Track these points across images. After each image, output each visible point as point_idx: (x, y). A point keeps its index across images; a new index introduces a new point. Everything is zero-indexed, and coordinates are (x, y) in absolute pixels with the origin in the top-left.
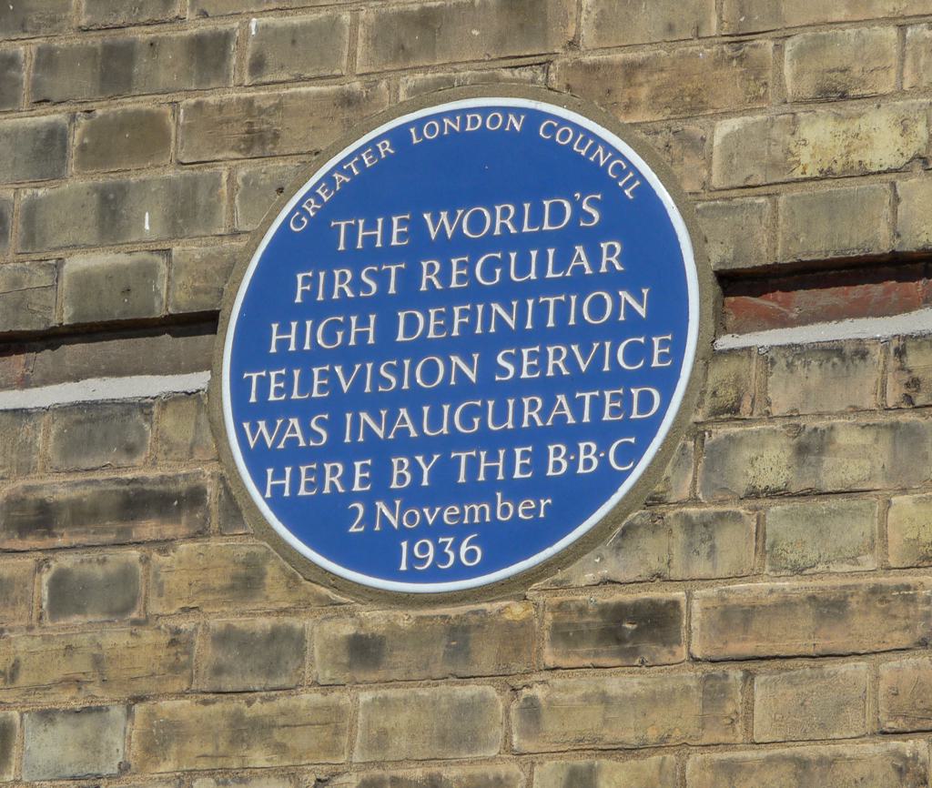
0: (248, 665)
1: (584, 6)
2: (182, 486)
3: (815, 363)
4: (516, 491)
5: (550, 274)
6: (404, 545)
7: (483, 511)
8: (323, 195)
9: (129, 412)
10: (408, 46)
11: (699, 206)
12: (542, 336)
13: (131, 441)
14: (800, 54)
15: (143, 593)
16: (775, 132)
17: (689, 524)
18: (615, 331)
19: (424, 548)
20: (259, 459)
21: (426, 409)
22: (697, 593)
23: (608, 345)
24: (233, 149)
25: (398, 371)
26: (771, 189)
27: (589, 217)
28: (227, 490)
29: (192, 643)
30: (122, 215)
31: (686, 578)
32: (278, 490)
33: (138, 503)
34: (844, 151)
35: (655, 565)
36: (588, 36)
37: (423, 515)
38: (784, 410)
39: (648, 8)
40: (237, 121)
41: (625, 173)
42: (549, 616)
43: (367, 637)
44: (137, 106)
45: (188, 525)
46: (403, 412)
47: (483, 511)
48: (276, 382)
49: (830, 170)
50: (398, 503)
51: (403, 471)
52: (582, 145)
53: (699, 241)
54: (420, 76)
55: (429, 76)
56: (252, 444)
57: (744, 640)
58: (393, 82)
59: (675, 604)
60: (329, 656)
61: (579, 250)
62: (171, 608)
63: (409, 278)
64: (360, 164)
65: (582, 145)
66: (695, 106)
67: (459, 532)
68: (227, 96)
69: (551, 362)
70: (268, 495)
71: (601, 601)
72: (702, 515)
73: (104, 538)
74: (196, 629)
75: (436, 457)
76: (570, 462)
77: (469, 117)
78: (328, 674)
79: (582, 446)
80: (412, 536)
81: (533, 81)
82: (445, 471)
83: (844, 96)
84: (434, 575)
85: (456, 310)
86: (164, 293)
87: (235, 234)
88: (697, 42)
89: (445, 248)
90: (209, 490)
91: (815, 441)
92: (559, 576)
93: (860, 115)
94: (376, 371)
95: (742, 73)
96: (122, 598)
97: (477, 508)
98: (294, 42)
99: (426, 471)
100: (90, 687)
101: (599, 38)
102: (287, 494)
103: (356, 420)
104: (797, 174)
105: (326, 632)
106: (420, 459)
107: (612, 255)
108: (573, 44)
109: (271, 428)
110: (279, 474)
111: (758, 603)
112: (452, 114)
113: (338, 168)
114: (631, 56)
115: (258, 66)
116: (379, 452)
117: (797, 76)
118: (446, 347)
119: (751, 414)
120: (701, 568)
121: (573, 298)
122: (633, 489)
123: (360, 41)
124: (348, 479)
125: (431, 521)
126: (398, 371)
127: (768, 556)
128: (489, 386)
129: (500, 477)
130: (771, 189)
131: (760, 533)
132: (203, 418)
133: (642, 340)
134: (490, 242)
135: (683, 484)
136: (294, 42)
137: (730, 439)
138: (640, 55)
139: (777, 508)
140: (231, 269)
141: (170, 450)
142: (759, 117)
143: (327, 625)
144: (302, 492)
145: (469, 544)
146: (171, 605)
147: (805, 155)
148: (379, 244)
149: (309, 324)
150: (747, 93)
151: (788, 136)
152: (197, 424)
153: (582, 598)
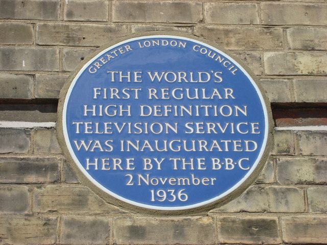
0: (82, 235)
1: (205, 9)
2: (46, 162)
3: (317, 138)
4: (199, 174)
5: (204, 97)
6: (152, 191)
7: (186, 181)
8: (103, 62)
9: (19, 133)
10: (134, 14)
11: (261, 80)
12: (202, 118)
13: (22, 144)
14: (293, 34)
15: (31, 203)
16: (288, 58)
17: (275, 191)
18: (234, 119)
19: (161, 193)
20: (82, 155)
21: (156, 142)
22: (283, 218)
23: (232, 124)
24: (61, 42)
25: (142, 126)
26: (290, 77)
27: (218, 79)
28: (68, 166)
29: (56, 225)
30: (12, 61)
31: (277, 211)
32: (92, 167)
33: (25, 168)
34: (317, 67)
35: (264, 207)
36: (208, 19)
37: (159, 180)
38: (309, 153)
39: (231, 13)
40: (62, 32)
41: (229, 66)
42: (220, 223)
43: (137, 227)
44: (17, 23)
45: (50, 178)
46: (146, 142)
47: (186, 181)
48: (88, 126)
49: (312, 73)
50: (148, 175)
51: (149, 163)
52: (211, 54)
53: (264, 93)
54: (140, 25)
55: (144, 25)
56: (79, 149)
57: (306, 237)
58: (129, 26)
59: (274, 221)
60: (120, 233)
61: (216, 90)
62: (44, 210)
63: (143, 94)
64: (117, 52)
65: (211, 55)
66: (255, 47)
67: (177, 188)
68: (57, 23)
69: (209, 129)
70: (88, 168)
71: (241, 218)
72: (281, 189)
73: (10, 181)
74: (57, 219)
75: (163, 159)
76: (222, 165)
77: (163, 41)
78: (120, 240)
79: (226, 160)
80: (156, 188)
81: (187, 32)
82: (167, 165)
83: (313, 49)
84: (166, 203)
85: (166, 107)
86: (32, 90)
87: (65, 72)
88: (252, 26)
89: (158, 85)
90: (59, 165)
91: (322, 165)
92: (222, 208)
93: (321, 56)
94: (132, 127)
95: (271, 38)
96: (20, 205)
97: (184, 180)
98: (85, 8)
99: (159, 164)
100: (6, 240)
101: (213, 21)
102: (96, 169)
103: (125, 143)
104: (299, 73)
105: (118, 223)
106: (156, 159)
107: (229, 93)
108: (202, 21)
109: (87, 143)
110: (92, 161)
111: (309, 223)
112: (154, 39)
113: (108, 52)
114: (226, 28)
115: (70, 14)
116: (139, 157)
117: (294, 41)
118: (163, 119)
119: (295, 154)
120: (283, 208)
121: (215, 107)
122: (250, 177)
123: (113, 11)
124: (124, 164)
125: (163, 183)
126: (142, 126)
127: (310, 206)
128: (182, 134)
129: (192, 168)
130: (290, 77)
131: (305, 197)
132: (54, 137)
133: (246, 123)
134: (176, 84)
135: (270, 177)
136: (85, 8)
137: (287, 161)
138: (231, 28)
139: (311, 188)
140: (63, 84)
141: (40, 149)
142: (281, 53)
143: (119, 221)
144: (103, 168)
145: (182, 192)
146: (44, 209)
147: (301, 67)
148: (129, 81)
149: (101, 106)
150: (274, 44)
151: (294, 61)
152: (52, 140)
153: (233, 217)
